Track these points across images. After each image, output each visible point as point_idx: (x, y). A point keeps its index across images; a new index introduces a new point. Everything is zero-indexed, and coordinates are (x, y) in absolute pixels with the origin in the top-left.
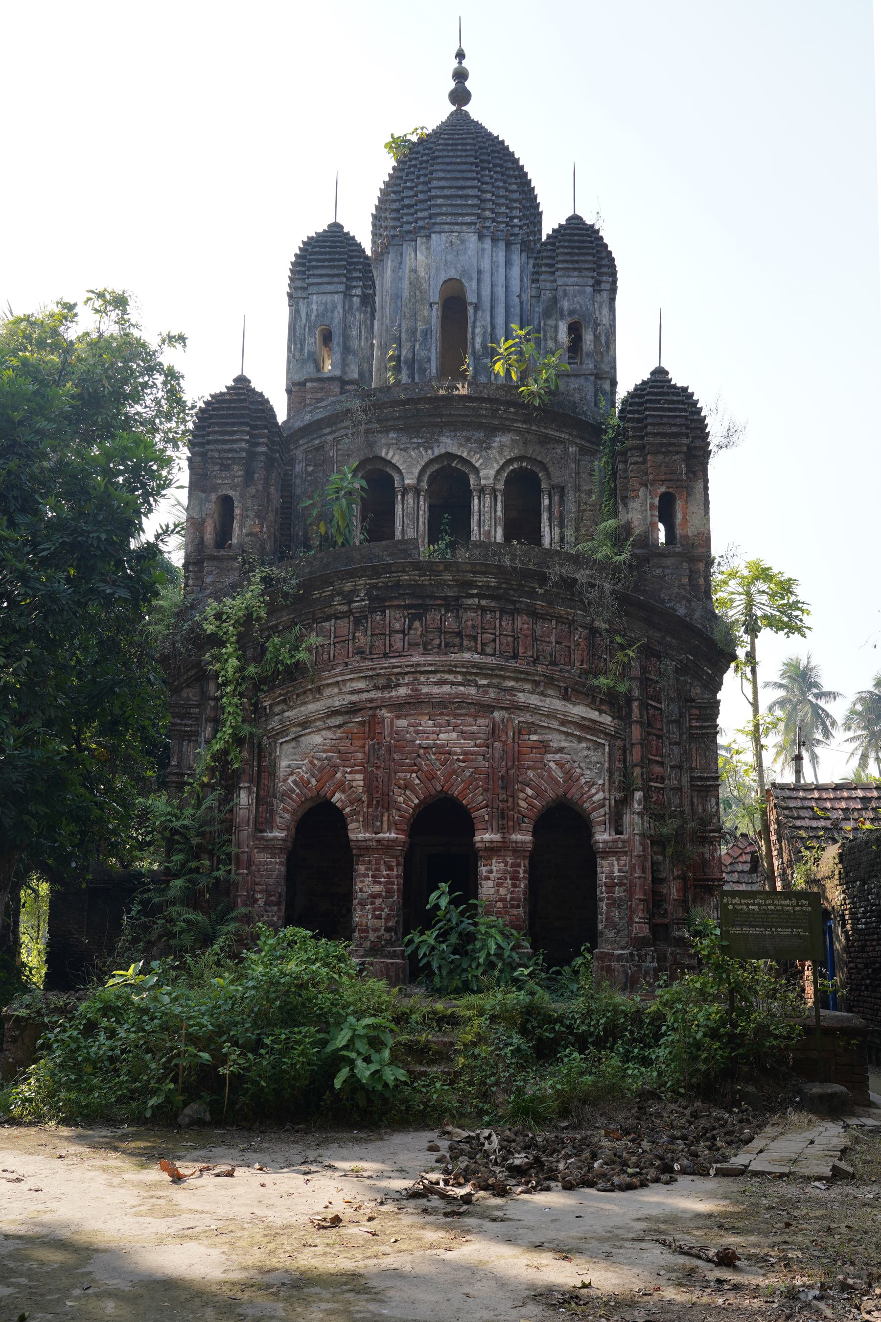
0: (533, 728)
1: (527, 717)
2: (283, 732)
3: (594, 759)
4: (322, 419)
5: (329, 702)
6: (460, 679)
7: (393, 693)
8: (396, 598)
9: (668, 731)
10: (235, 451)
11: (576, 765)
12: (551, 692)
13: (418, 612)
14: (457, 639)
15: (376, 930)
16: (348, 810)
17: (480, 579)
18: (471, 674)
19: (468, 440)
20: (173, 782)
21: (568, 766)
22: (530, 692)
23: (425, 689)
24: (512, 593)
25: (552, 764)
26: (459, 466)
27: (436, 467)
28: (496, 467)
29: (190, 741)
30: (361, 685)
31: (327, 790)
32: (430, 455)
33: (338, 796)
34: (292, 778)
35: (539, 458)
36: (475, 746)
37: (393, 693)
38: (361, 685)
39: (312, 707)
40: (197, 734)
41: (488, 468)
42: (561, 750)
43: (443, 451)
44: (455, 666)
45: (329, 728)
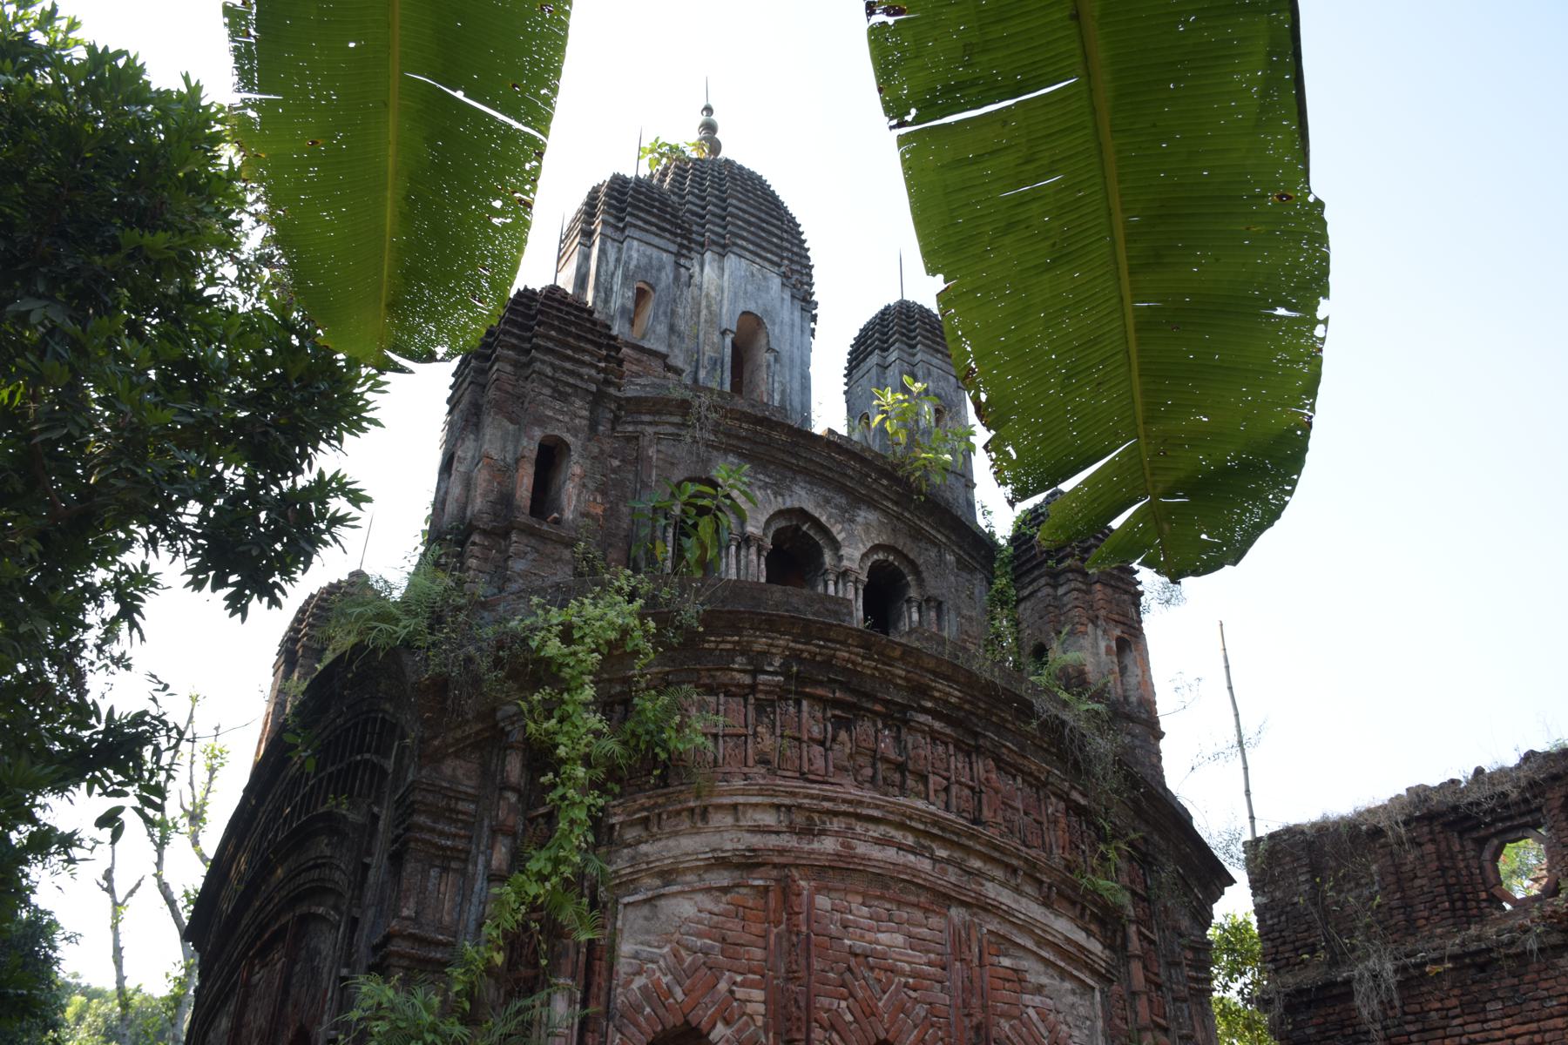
0: (1004, 944)
1: (993, 925)
2: (629, 884)
3: (1082, 1011)
4: (646, 399)
5: (715, 840)
6: (910, 840)
7: (816, 845)
8: (821, 683)
9: (1170, 978)
10: (580, 376)
11: (1061, 1017)
12: (1028, 889)
13: (845, 716)
14: (903, 773)
17: (941, 685)
18: (927, 834)
19: (828, 501)
20: (401, 956)
21: (1051, 1017)
22: (1002, 884)
23: (861, 849)
24: (975, 720)
25: (1031, 1012)
26: (811, 533)
27: (783, 523)
28: (863, 550)
29: (445, 869)
30: (769, 819)
31: (702, 1016)
32: (779, 504)
33: (720, 1026)
34: (639, 982)
35: (911, 556)
36: (930, 964)
37: (816, 845)
38: (769, 819)
39: (688, 843)
40: (466, 857)
41: (855, 543)
42: (1039, 989)
43: (796, 505)
44: (910, 818)
45: (708, 890)
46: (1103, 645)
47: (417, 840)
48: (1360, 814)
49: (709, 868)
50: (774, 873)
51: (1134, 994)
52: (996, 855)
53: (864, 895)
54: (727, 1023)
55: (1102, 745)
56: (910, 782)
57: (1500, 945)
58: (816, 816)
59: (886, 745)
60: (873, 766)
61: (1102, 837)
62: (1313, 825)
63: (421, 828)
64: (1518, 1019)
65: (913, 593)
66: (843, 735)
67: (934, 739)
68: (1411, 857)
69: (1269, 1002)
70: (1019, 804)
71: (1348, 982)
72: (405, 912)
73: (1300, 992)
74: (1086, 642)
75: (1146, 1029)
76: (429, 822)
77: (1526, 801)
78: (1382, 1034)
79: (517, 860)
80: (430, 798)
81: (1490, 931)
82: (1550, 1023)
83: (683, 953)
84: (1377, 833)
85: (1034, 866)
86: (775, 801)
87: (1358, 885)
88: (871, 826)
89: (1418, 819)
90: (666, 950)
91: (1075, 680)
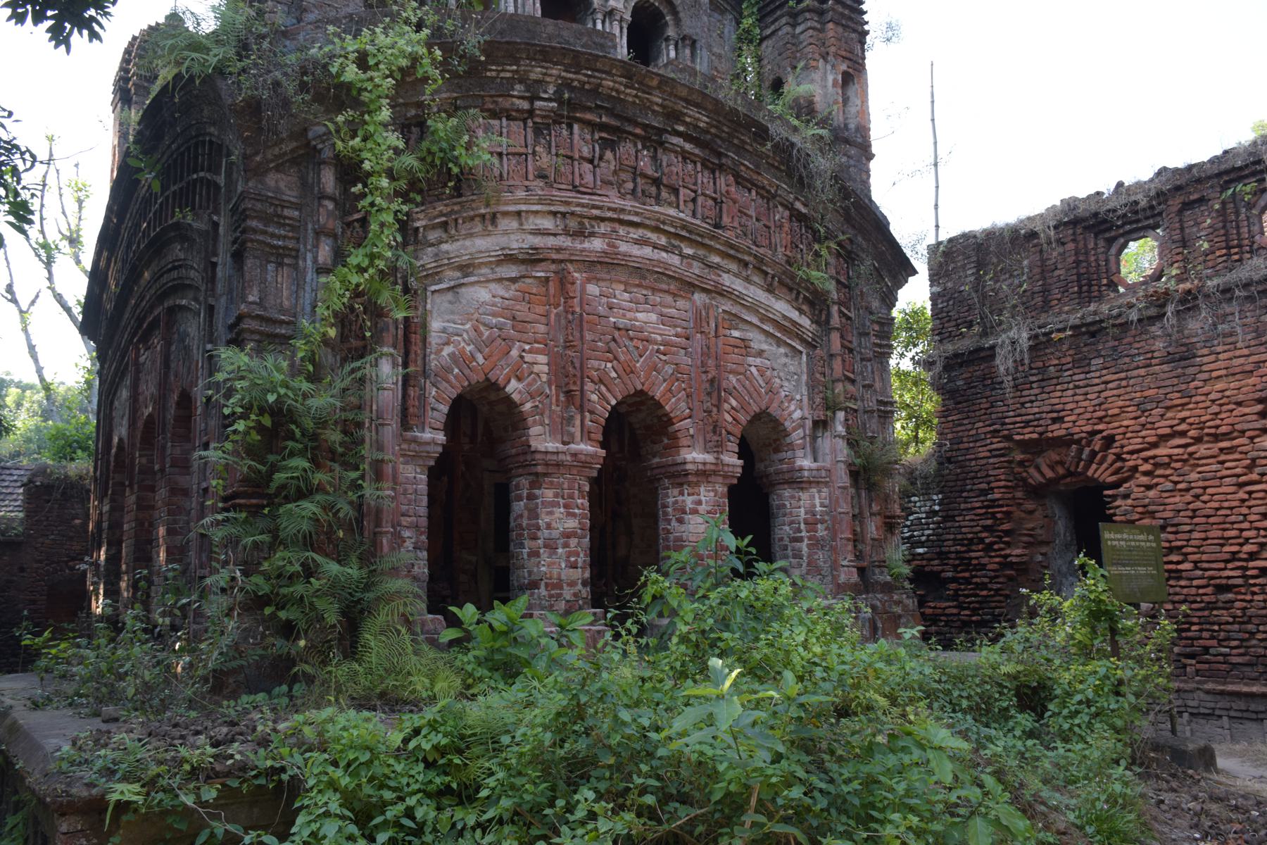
1: (727, 306)
2: (435, 276)
3: (792, 369)
5: (503, 241)
6: (663, 241)
7: (586, 245)
8: (589, 109)
9: (860, 345)
11: (775, 373)
12: (756, 279)
13: (611, 137)
15: (572, 584)
16: (528, 406)
17: (692, 112)
18: (677, 236)
20: (253, 332)
21: (768, 373)
22: (735, 275)
23: (623, 247)
24: (719, 142)
25: (753, 370)
29: (280, 265)
31: (499, 375)
33: (514, 383)
34: (447, 351)
36: (677, 335)
37: (586, 245)
38: (547, 223)
39: (481, 243)
40: (296, 254)
42: (760, 353)
44: (664, 223)
45: (500, 280)
46: (830, 78)
47: (252, 241)
48: (1022, 221)
49: (499, 263)
50: (553, 267)
51: (832, 356)
52: (732, 252)
53: (626, 284)
54: (519, 379)
55: (823, 164)
56: (664, 194)
57: (1110, 317)
58: (586, 221)
59: (645, 164)
60: (634, 180)
61: (817, 238)
62: (984, 231)
63: (255, 231)
64: (1113, 370)
65: (671, 32)
66: (609, 155)
67: (684, 159)
68: (1055, 254)
69: (933, 363)
70: (752, 212)
71: (993, 348)
72: (251, 299)
73: (956, 355)
74: (816, 76)
75: (838, 380)
76: (261, 226)
77: (1152, 207)
78: (1012, 384)
79: (340, 256)
80: (259, 206)
81: (1105, 308)
82: (1135, 373)
83: (482, 328)
84: (1033, 235)
85: (761, 261)
86: (552, 208)
87: (1011, 276)
88: (632, 230)
89: (1066, 224)
90: (468, 326)
91: (805, 109)
